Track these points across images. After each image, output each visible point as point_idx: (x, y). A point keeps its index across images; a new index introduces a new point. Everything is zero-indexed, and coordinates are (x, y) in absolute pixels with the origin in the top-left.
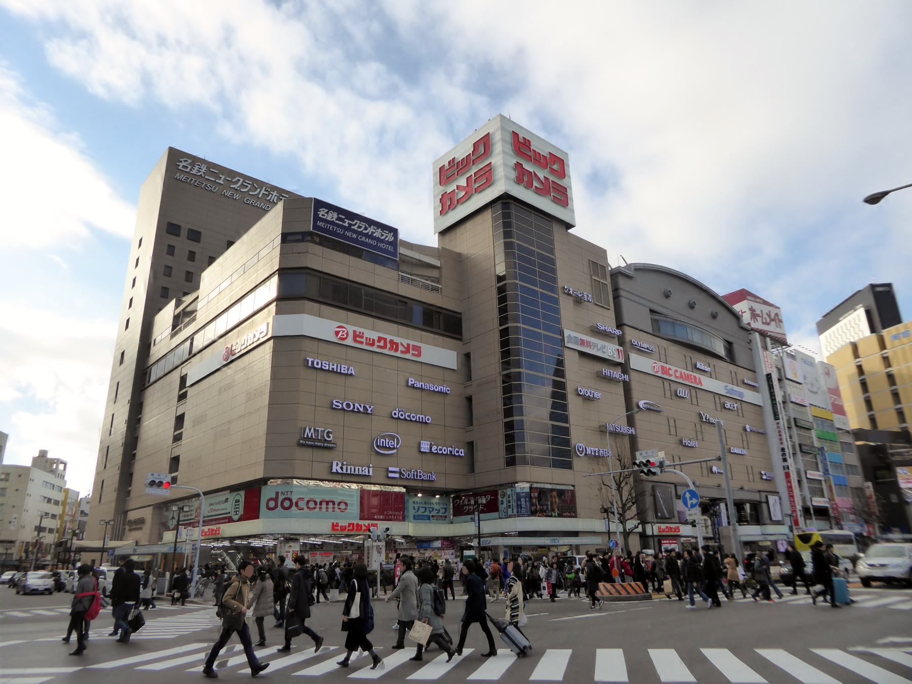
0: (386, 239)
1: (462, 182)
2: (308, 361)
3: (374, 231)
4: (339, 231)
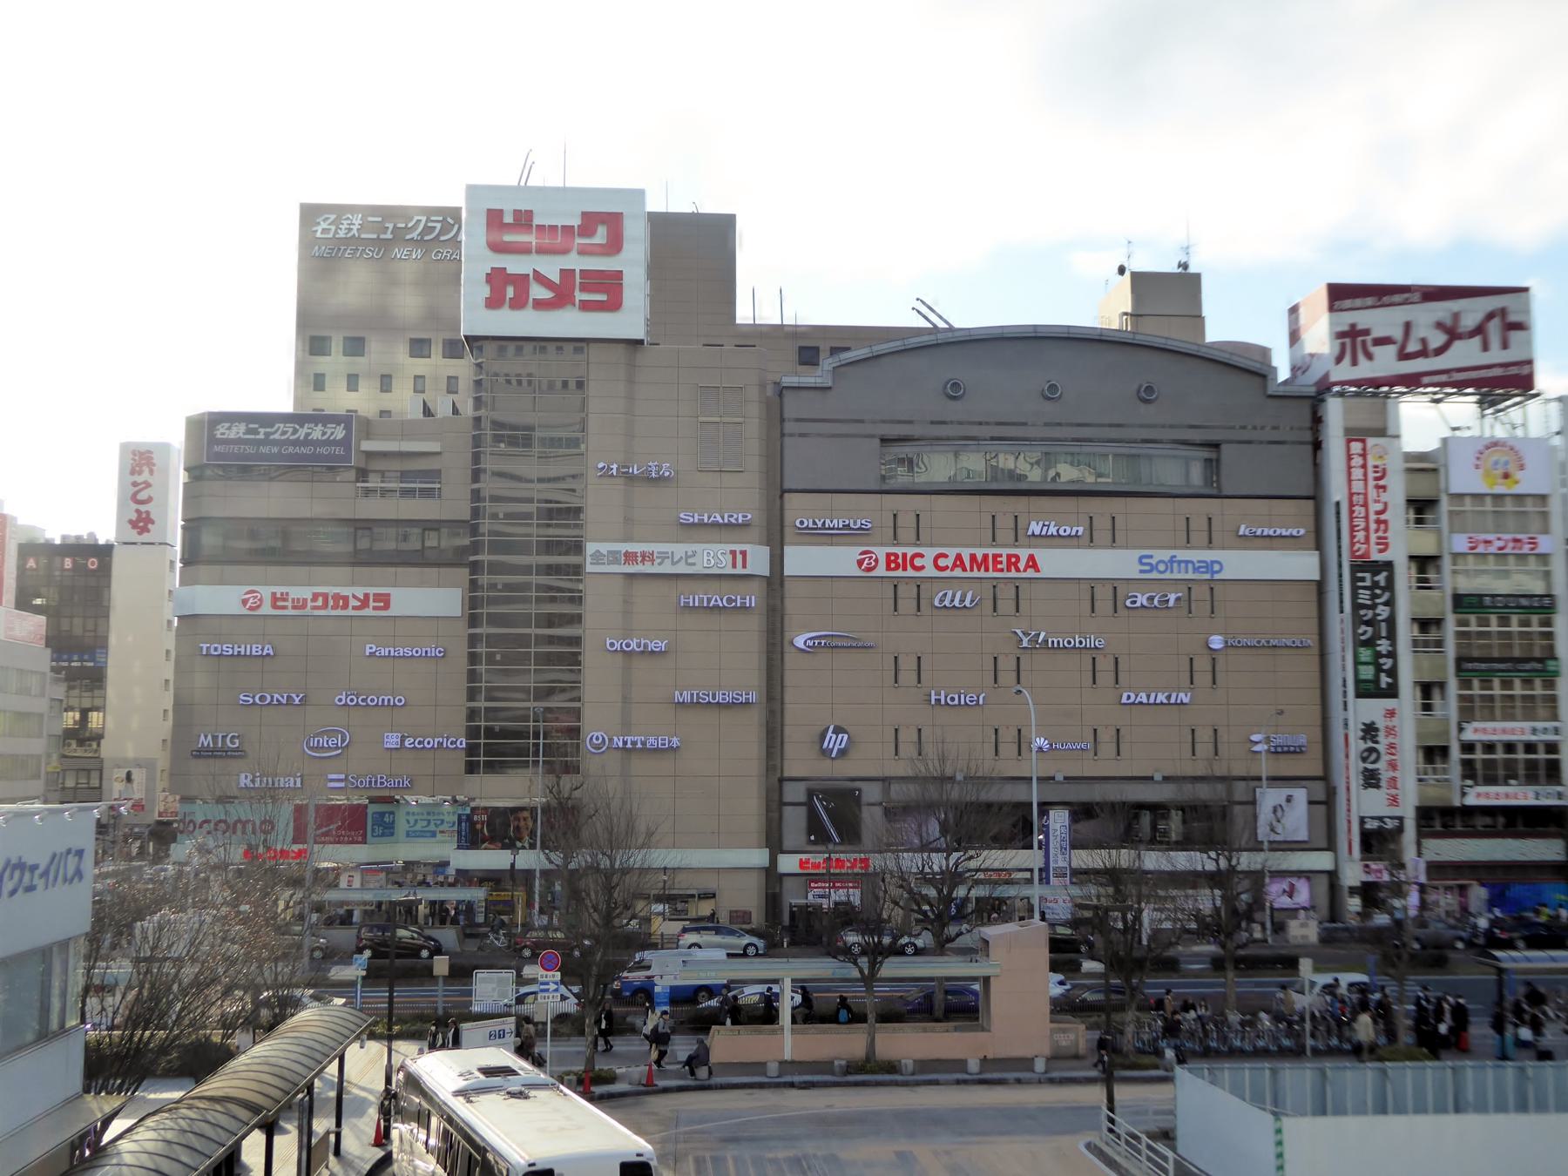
2: (202, 648)
4: (250, 450)
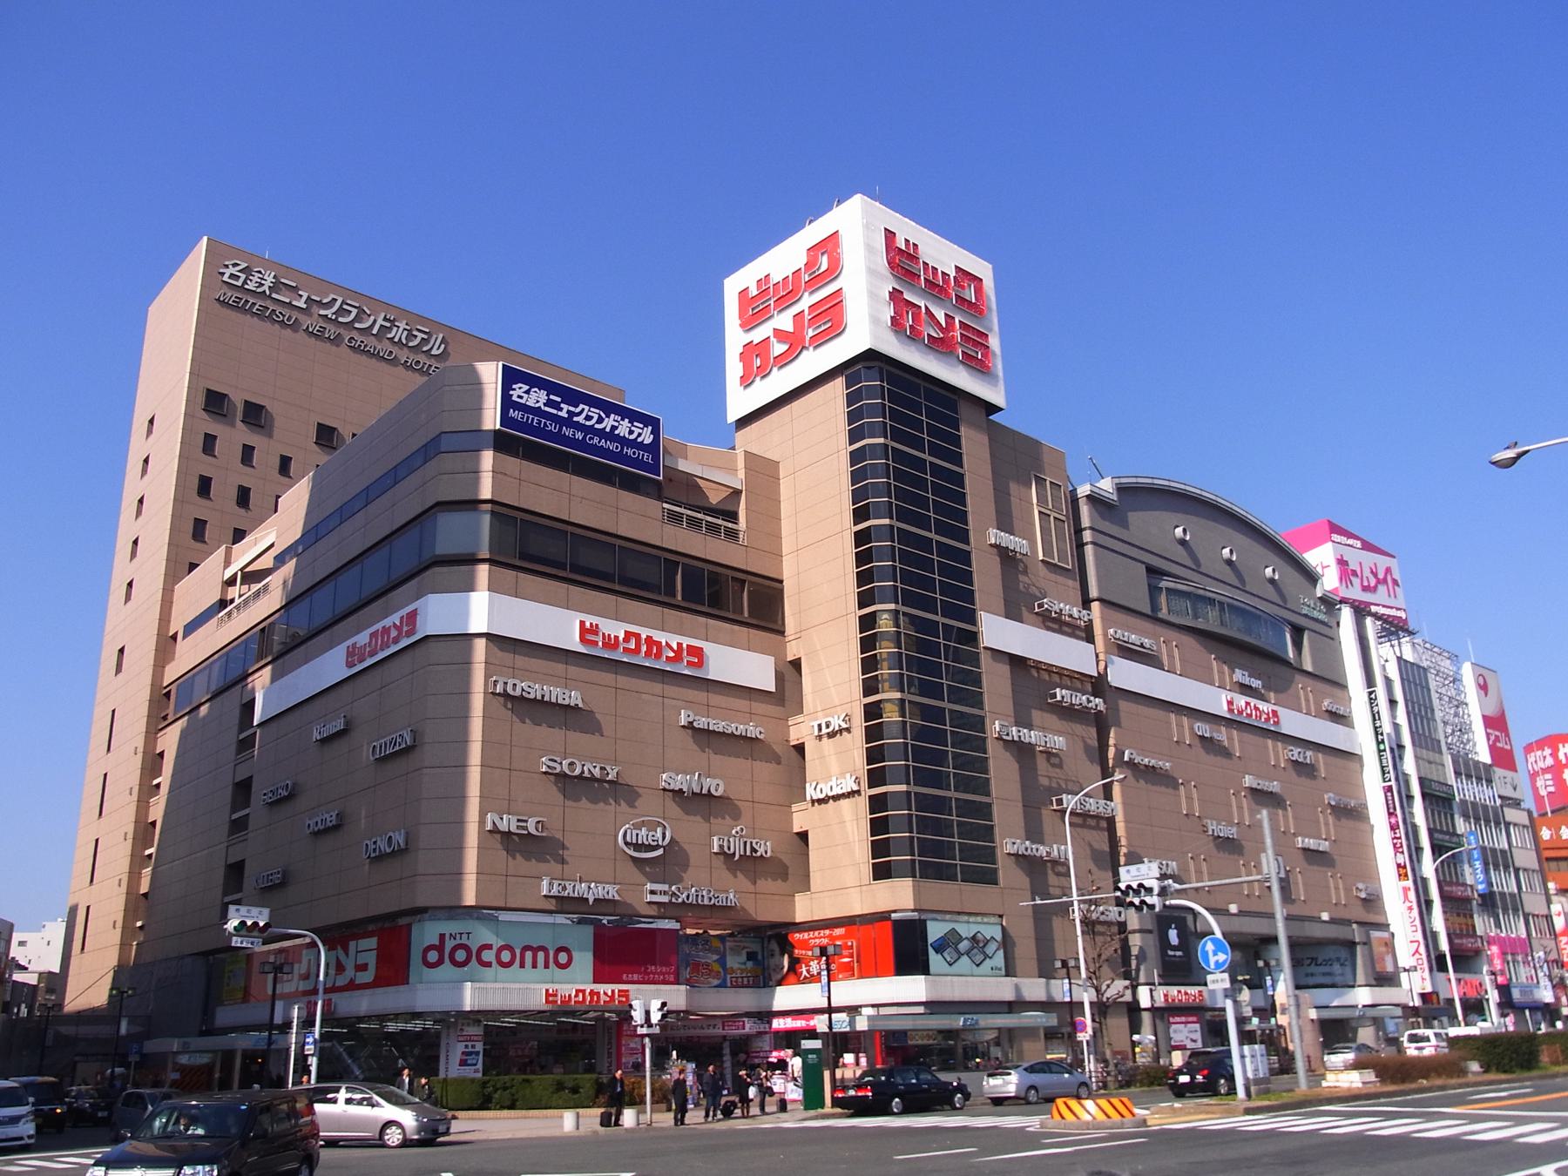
0: (639, 440)
1: (784, 321)
3: (616, 424)
4: (552, 427)
